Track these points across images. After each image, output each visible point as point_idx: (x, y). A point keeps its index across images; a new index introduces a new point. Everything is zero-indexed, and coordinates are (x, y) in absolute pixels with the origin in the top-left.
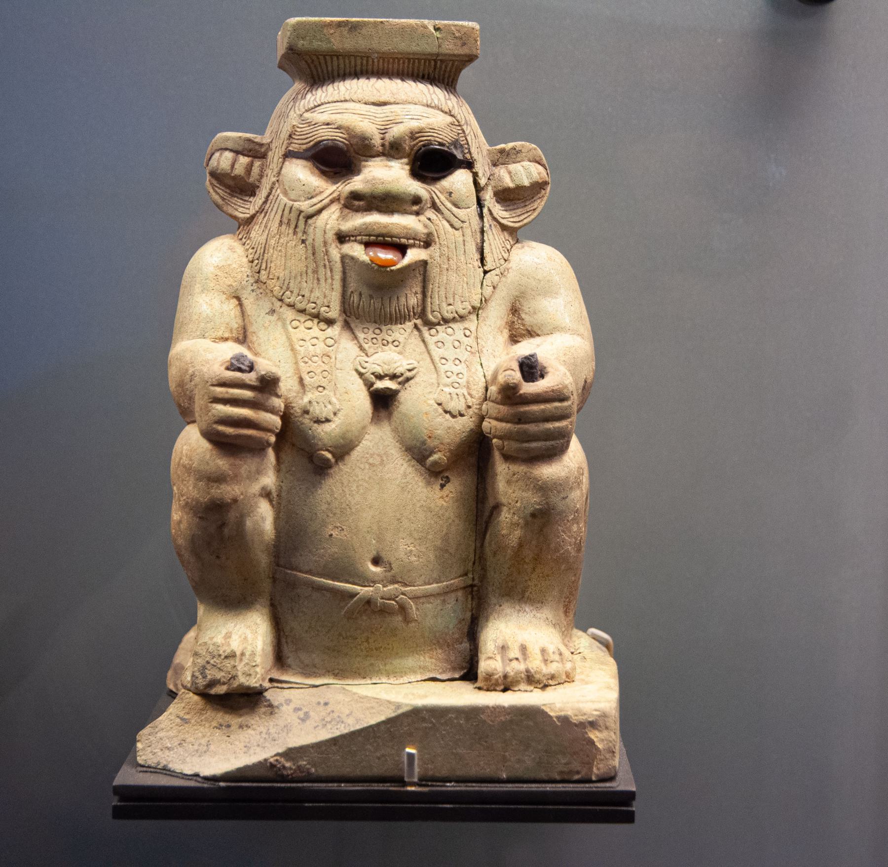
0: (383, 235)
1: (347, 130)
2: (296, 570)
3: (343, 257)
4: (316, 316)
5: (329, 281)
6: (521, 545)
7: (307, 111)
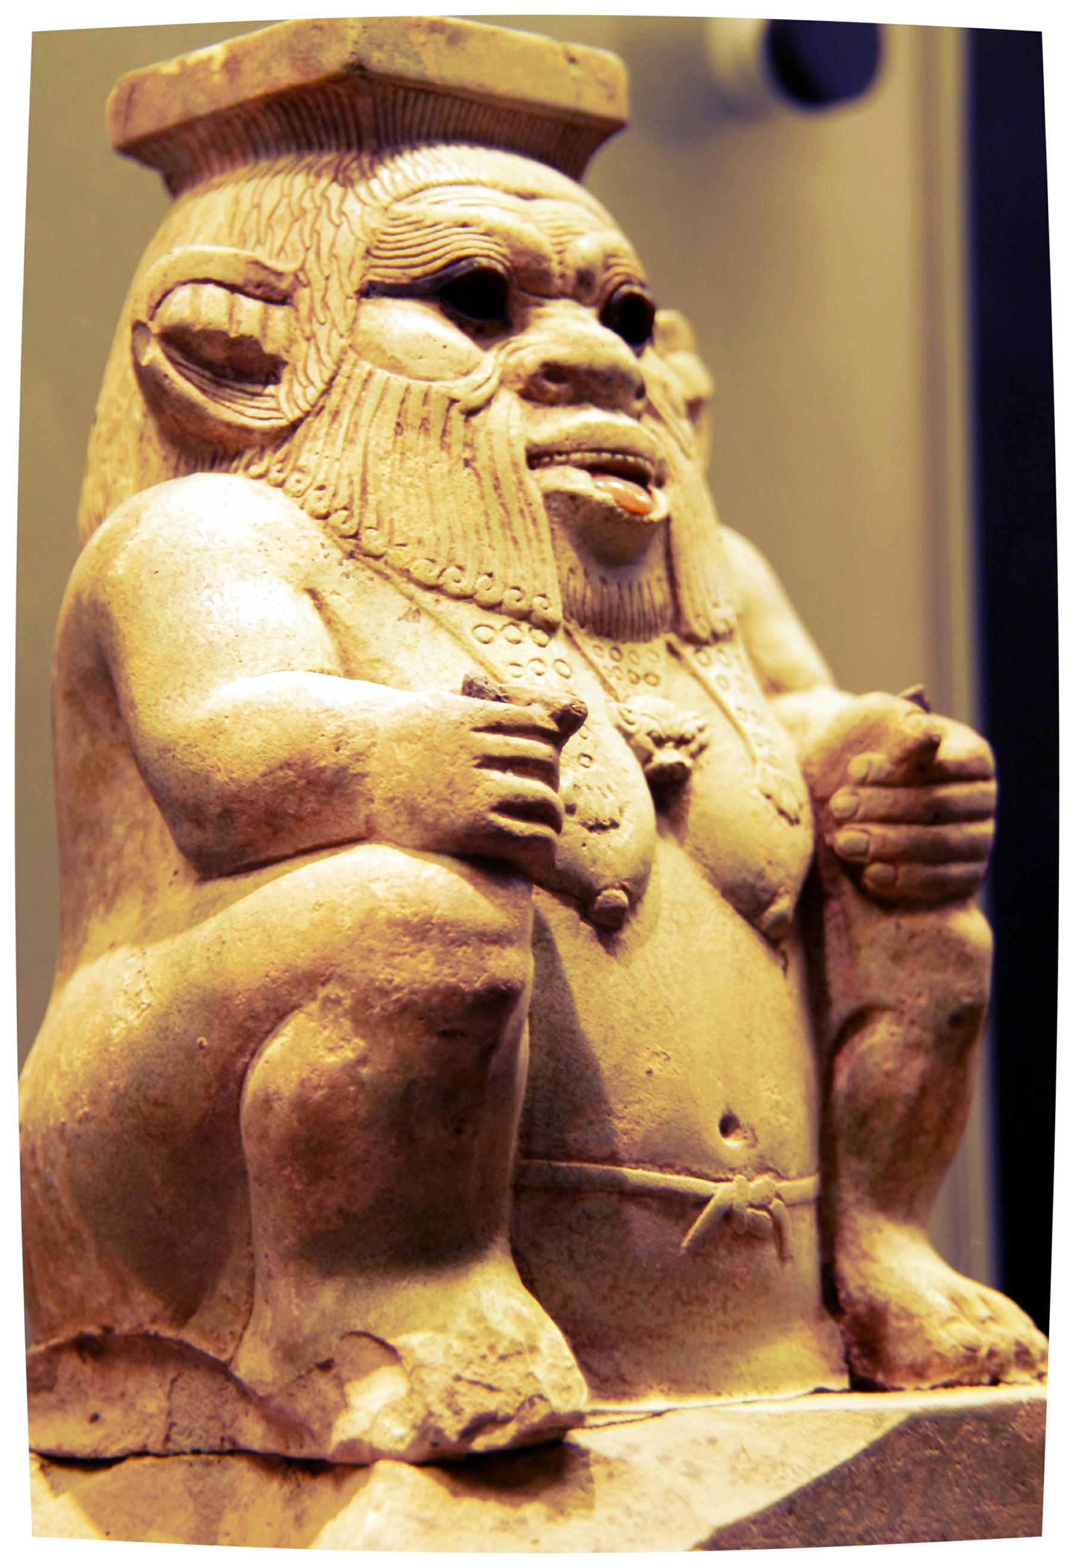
0: (624, 452)
1: (507, 237)
2: (580, 1159)
3: (549, 496)
4: (524, 616)
5: (535, 543)
6: (923, 1091)
7: (398, 200)
